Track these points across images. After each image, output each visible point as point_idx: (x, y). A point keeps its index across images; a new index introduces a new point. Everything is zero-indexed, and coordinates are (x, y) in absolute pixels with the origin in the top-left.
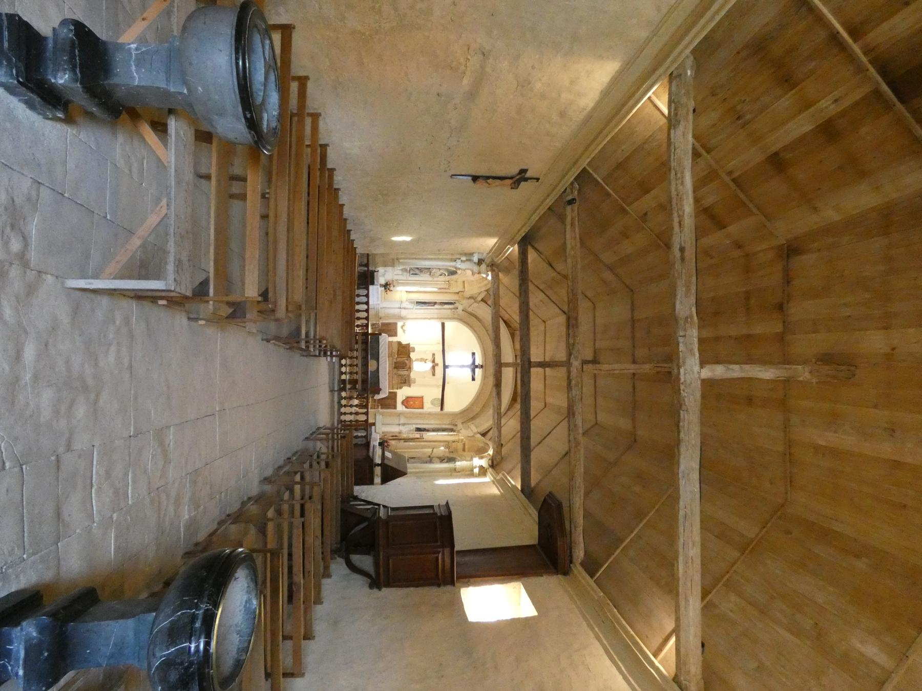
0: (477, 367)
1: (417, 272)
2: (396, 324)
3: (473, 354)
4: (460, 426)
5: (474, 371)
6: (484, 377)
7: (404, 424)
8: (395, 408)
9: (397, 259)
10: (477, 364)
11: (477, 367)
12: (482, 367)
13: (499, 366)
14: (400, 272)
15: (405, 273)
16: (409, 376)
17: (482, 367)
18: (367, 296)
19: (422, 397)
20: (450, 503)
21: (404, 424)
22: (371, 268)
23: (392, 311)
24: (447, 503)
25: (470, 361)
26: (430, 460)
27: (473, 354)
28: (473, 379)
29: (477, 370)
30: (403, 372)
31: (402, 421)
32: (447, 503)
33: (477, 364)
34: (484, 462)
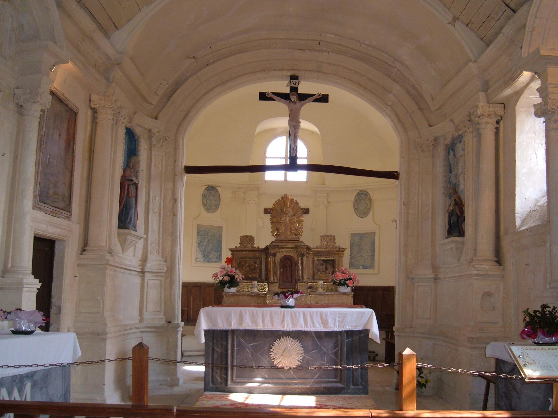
0: (294, 89)
2: (187, 286)
3: (263, 96)
5: (303, 97)
6: (320, 73)
10: (287, 90)
12: (294, 78)
16: (317, 253)
17: (294, 78)
19: (353, 235)
23: (153, 294)
25: (281, 106)
27: (263, 96)
28: (324, 99)
29: (303, 88)
30: (306, 268)
33: (287, 90)
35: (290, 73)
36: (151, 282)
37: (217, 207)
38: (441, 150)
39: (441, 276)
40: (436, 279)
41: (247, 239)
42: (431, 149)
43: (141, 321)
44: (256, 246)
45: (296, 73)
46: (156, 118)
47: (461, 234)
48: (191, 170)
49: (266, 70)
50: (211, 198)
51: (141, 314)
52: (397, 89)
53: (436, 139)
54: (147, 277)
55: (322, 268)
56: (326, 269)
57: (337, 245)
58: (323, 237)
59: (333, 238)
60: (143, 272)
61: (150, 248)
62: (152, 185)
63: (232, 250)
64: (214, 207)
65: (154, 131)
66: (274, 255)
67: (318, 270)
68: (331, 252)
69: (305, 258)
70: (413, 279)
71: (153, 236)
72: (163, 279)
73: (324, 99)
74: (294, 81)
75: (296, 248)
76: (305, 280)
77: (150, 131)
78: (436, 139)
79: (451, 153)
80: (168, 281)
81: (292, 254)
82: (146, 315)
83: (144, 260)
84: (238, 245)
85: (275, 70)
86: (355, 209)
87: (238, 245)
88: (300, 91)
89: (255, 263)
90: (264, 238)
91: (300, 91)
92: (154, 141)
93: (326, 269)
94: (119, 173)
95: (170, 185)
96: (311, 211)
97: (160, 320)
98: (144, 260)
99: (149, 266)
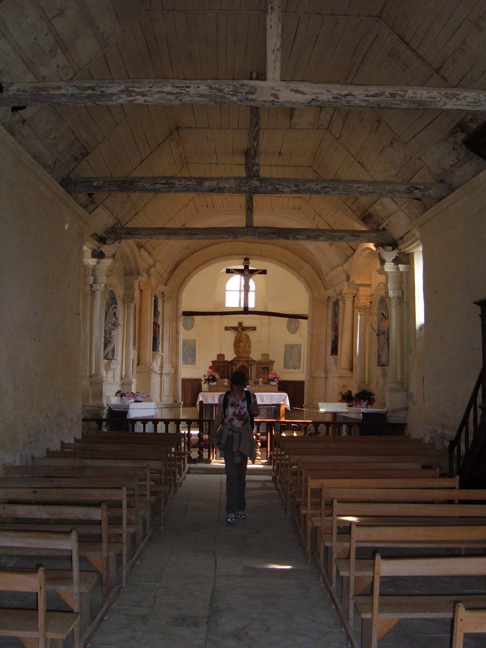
0: (246, 267)
1: (110, 348)
3: (228, 271)
4: (331, 293)
5: (252, 272)
6: (262, 256)
7: (326, 372)
8: (302, 383)
9: (91, 377)
11: (246, 267)
12: (246, 260)
13: (251, 230)
14: (110, 374)
15: (112, 366)
16: (259, 363)
17: (246, 260)
18: (144, 421)
19: (287, 346)
20: (478, 298)
21: (326, 372)
22: (104, 417)
23: (167, 386)
24: (479, 303)
26: (383, 334)
27: (228, 271)
28: (264, 272)
31: (323, 375)
32: (479, 303)
33: (242, 267)
34: (390, 255)
35: (244, 257)
36: (165, 379)
37: (192, 326)
38: (331, 304)
39: (328, 376)
40: (326, 378)
41: (221, 356)
42: (326, 303)
43: (161, 401)
44: (226, 359)
45: (248, 257)
46: (166, 285)
47: (337, 354)
48: (186, 314)
49: (230, 255)
50: (188, 320)
51: (161, 397)
52: (307, 266)
53: (329, 297)
54: (164, 376)
55: (262, 372)
56: (264, 372)
57: (270, 359)
58: (263, 355)
59: (268, 355)
60: (161, 374)
61: (164, 360)
62: (165, 324)
63: (212, 362)
64: (190, 326)
65: (165, 293)
66: (236, 365)
67: (260, 373)
68: (267, 363)
69: (252, 367)
70: (314, 377)
71: (166, 354)
72: (172, 378)
73: (264, 272)
74: (247, 262)
75: (248, 361)
76: (253, 378)
77: (163, 293)
78: (329, 297)
79: (337, 306)
80: (174, 379)
81: (245, 364)
82: (163, 398)
83: (162, 367)
84: (216, 359)
85: (235, 255)
86: (288, 328)
87: (216, 359)
88: (250, 268)
89: (226, 369)
90: (230, 356)
91: (250, 268)
92: (165, 299)
93: (264, 372)
94: (152, 320)
95: (175, 323)
96: (258, 328)
97: (170, 401)
98: (162, 367)
99: (165, 370)
